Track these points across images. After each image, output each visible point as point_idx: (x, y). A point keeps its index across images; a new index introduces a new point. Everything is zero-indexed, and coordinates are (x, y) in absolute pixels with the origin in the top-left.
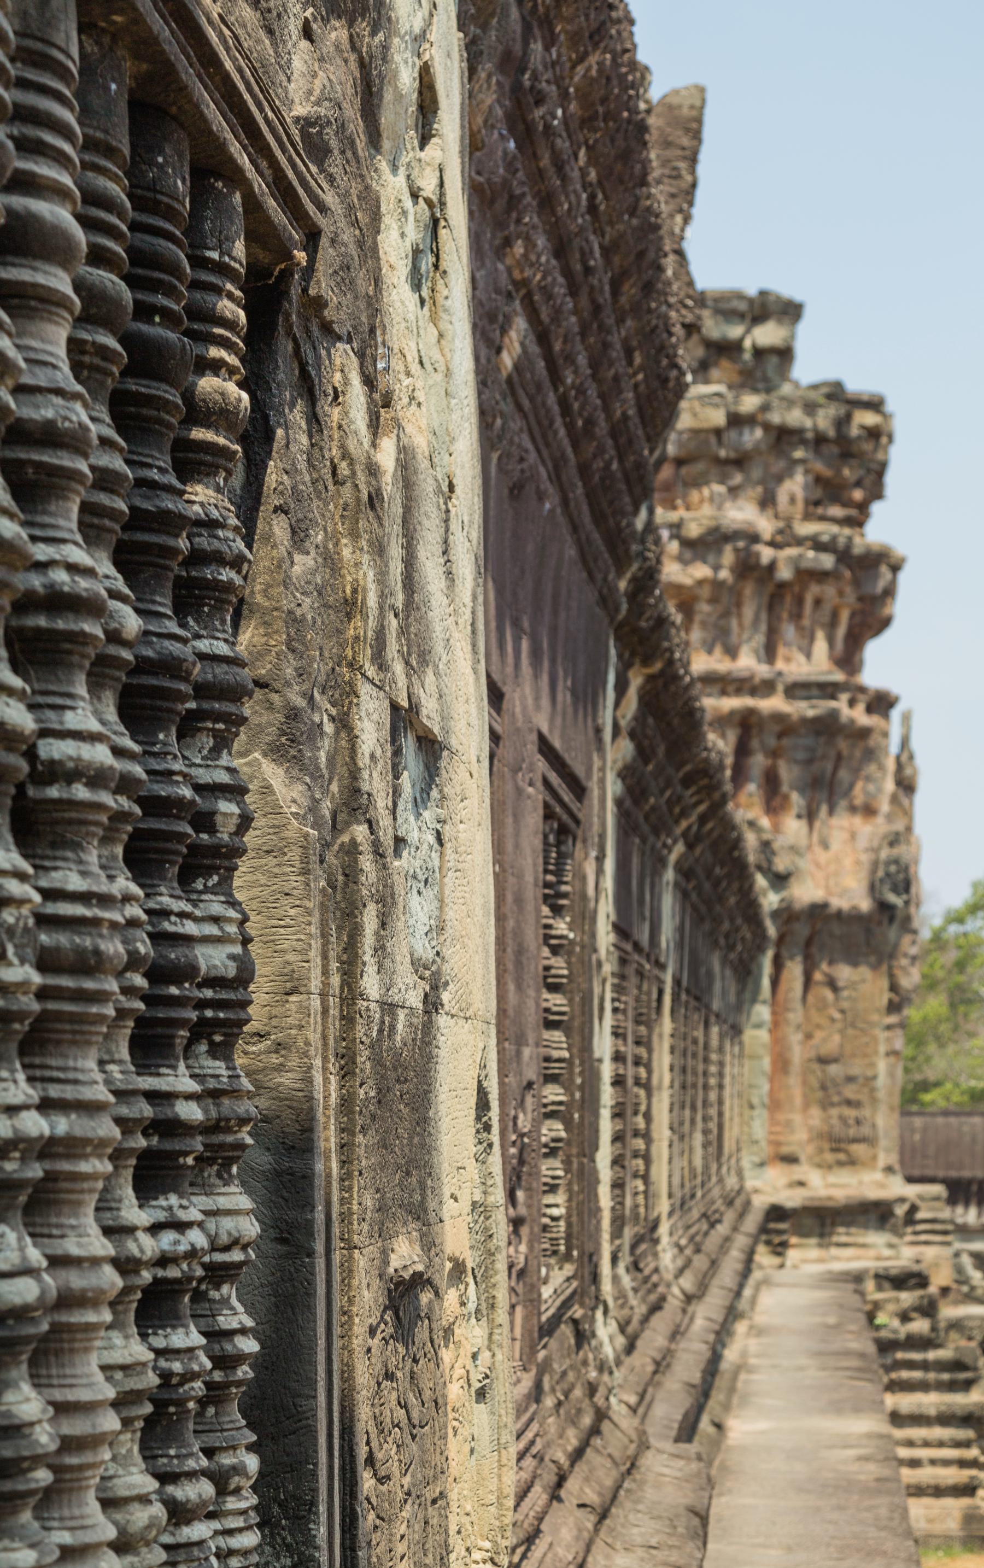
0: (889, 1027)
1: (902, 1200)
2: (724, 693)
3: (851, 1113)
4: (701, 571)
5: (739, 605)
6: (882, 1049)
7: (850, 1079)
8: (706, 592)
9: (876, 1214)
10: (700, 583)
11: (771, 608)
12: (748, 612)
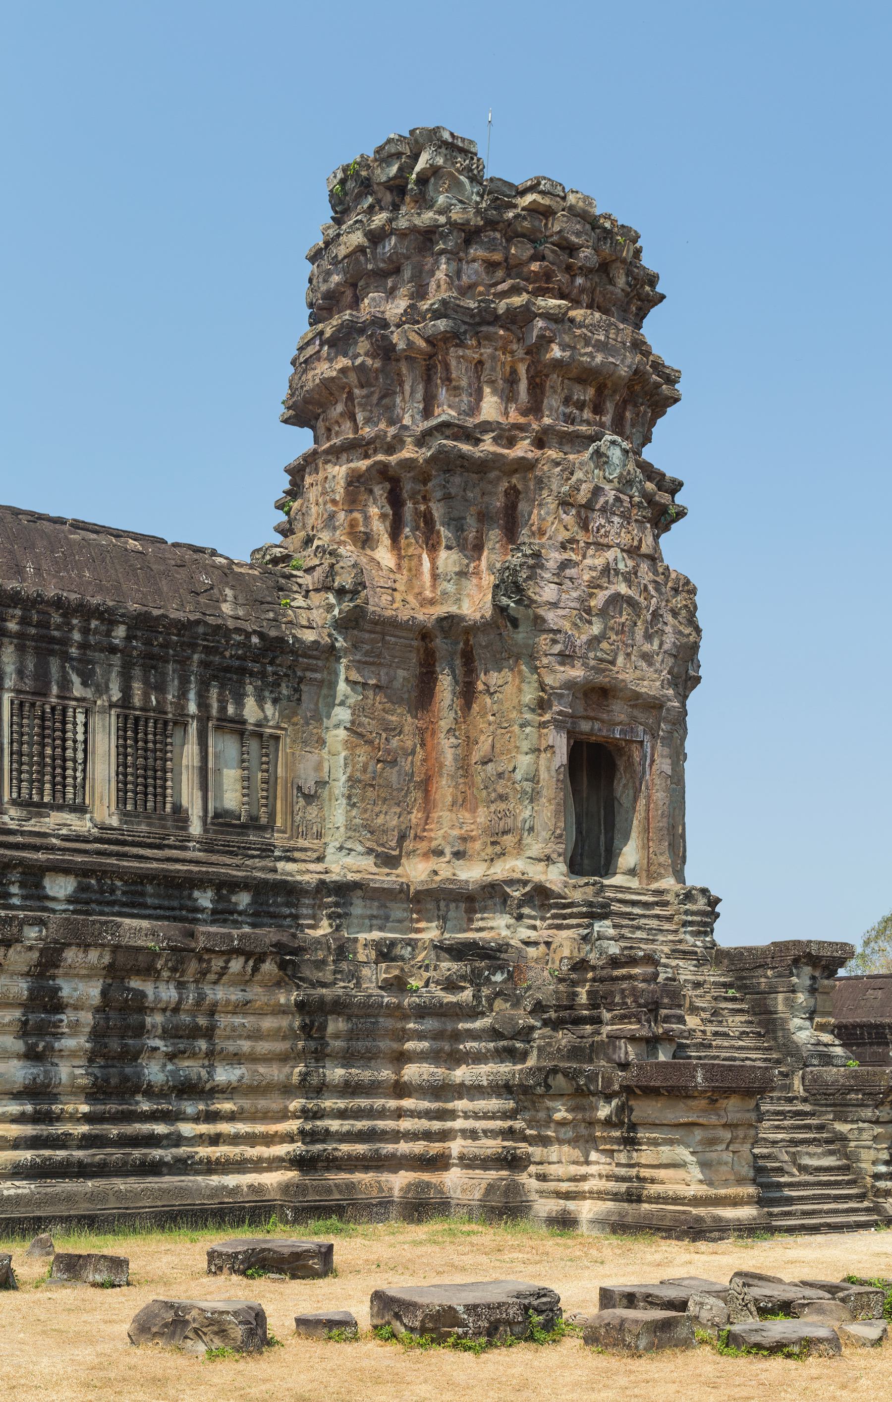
0: (543, 725)
1: (525, 883)
2: (367, 456)
3: (502, 806)
4: (343, 362)
5: (401, 384)
6: (525, 746)
7: (500, 775)
8: (353, 378)
9: (492, 895)
10: (343, 371)
11: (428, 380)
12: (407, 388)
